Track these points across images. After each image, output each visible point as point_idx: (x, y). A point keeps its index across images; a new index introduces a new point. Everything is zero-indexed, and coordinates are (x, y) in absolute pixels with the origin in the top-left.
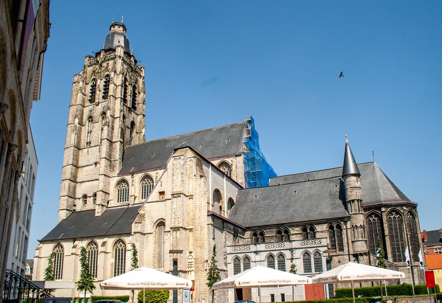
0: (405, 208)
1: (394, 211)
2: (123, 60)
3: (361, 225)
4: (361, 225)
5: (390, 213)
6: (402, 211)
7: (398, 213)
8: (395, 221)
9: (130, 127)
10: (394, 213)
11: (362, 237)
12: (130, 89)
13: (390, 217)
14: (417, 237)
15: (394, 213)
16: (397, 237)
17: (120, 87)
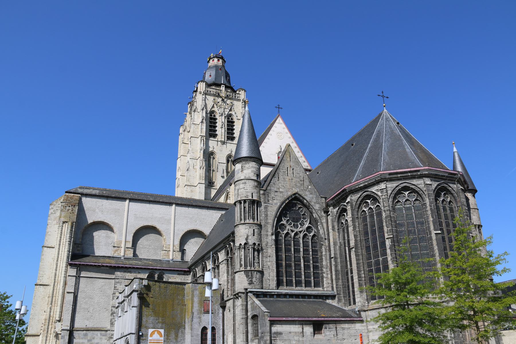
0: (382, 186)
1: (368, 197)
2: (206, 94)
3: (241, 244)
4: (241, 244)
5: (363, 201)
6: (379, 194)
7: (375, 199)
8: (372, 216)
9: (225, 161)
10: (369, 201)
11: (241, 266)
12: (221, 121)
13: (364, 211)
14: (431, 239)
15: (369, 201)
16: (375, 247)
17: (200, 125)
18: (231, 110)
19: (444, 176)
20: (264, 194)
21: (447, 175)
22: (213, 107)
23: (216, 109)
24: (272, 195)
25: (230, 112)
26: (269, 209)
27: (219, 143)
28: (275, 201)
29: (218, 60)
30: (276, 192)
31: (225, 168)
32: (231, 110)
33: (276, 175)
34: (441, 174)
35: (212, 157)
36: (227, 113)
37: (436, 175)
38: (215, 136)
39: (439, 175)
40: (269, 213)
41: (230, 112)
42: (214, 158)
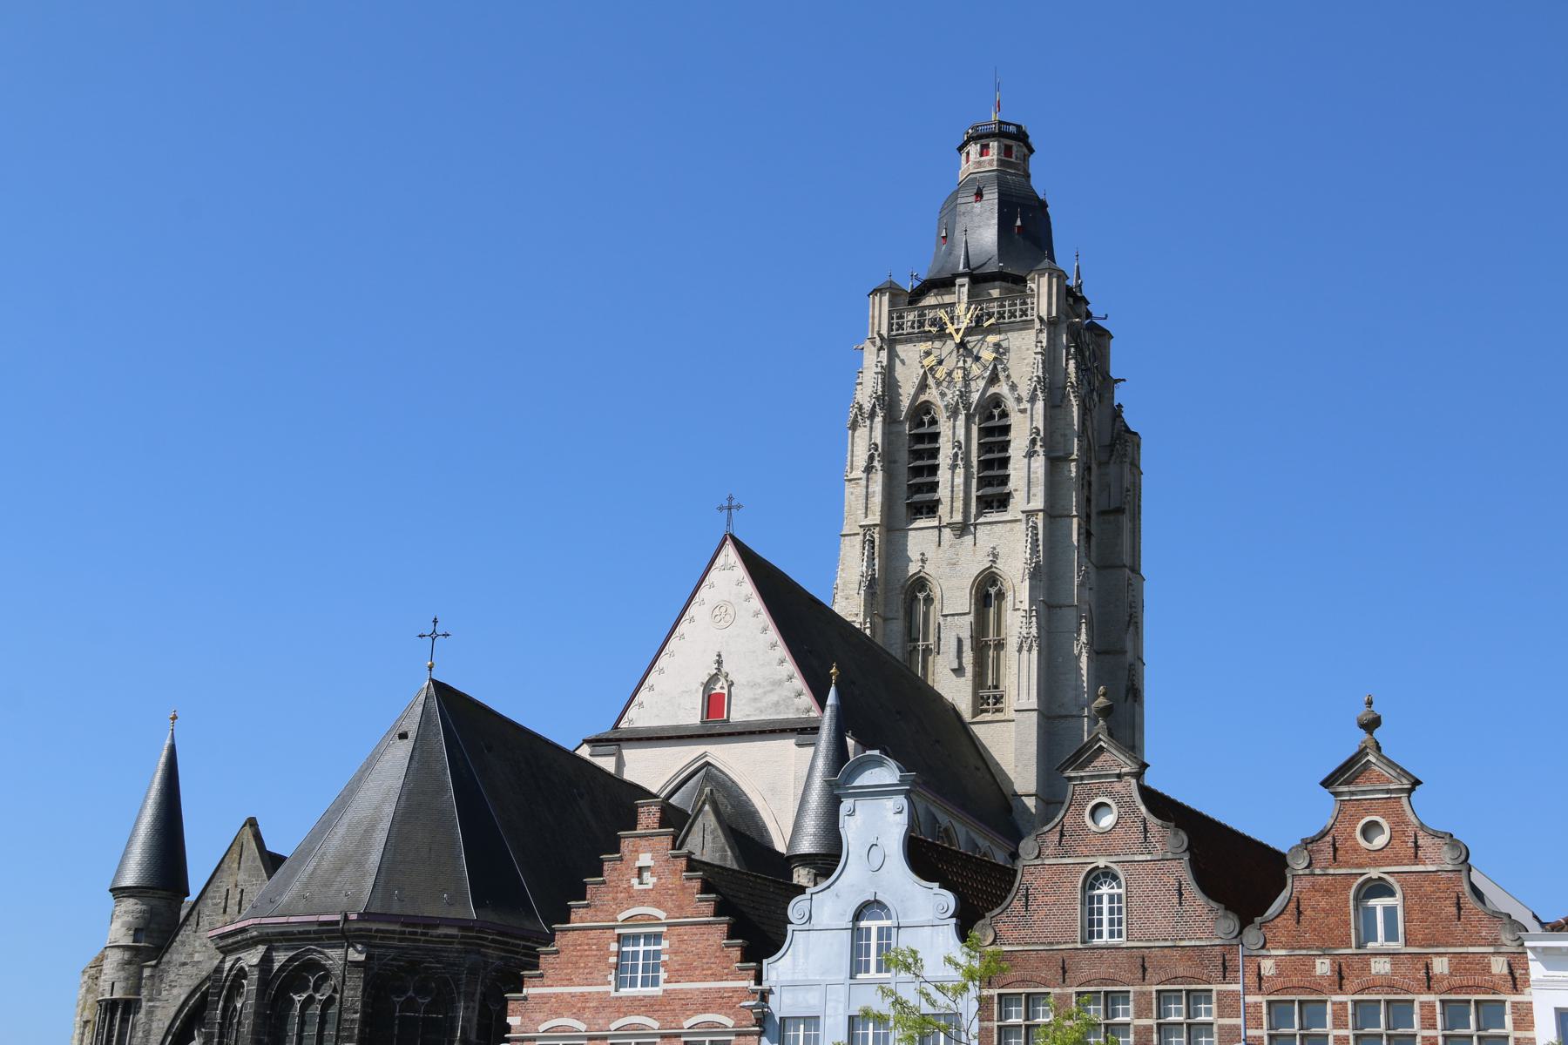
18: (993, 379)
19: (309, 932)
20: (152, 976)
21: (315, 928)
22: (923, 386)
23: (932, 395)
24: (172, 977)
25: (992, 390)
26: (159, 1014)
27: (947, 532)
28: (175, 991)
29: (984, 150)
30: (184, 964)
31: (966, 635)
32: (993, 379)
33: (193, 920)
34: (295, 930)
35: (921, 596)
36: (975, 397)
37: (282, 934)
38: (931, 508)
39: (292, 933)
40: (154, 1025)
41: (992, 390)
42: (929, 600)
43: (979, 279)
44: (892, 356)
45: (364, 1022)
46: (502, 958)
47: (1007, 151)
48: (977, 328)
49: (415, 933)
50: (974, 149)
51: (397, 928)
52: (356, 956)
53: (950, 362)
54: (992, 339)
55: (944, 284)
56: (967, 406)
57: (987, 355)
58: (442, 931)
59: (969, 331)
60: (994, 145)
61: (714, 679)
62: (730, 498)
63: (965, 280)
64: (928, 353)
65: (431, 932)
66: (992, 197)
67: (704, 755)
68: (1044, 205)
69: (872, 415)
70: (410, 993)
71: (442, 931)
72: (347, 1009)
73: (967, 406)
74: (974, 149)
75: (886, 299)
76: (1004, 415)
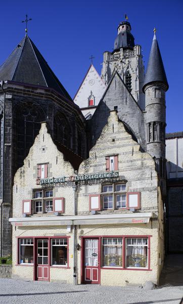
18: (128, 68)
32: (128, 68)
36: (124, 72)
43: (125, 49)
44: (108, 65)
45: (14, 121)
46: (59, 107)
47: (127, 27)
48: (125, 58)
49: (29, 91)
50: (121, 27)
51: (22, 88)
52: (10, 96)
53: (120, 65)
54: (127, 60)
55: (118, 50)
56: (123, 73)
57: (127, 62)
58: (39, 91)
59: (123, 59)
60: (125, 26)
61: (90, 97)
62: (92, 56)
63: (122, 49)
64: (115, 63)
65: (35, 91)
66: (125, 34)
67: (90, 112)
68: (134, 39)
69: (105, 76)
70: (29, 114)
71: (39, 91)
72: (7, 116)
73: (123, 73)
74: (121, 27)
75: (107, 53)
76: (130, 75)
